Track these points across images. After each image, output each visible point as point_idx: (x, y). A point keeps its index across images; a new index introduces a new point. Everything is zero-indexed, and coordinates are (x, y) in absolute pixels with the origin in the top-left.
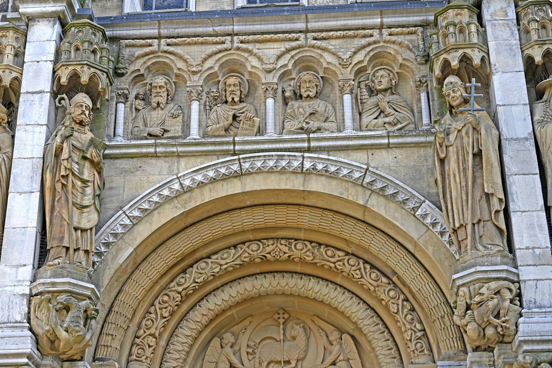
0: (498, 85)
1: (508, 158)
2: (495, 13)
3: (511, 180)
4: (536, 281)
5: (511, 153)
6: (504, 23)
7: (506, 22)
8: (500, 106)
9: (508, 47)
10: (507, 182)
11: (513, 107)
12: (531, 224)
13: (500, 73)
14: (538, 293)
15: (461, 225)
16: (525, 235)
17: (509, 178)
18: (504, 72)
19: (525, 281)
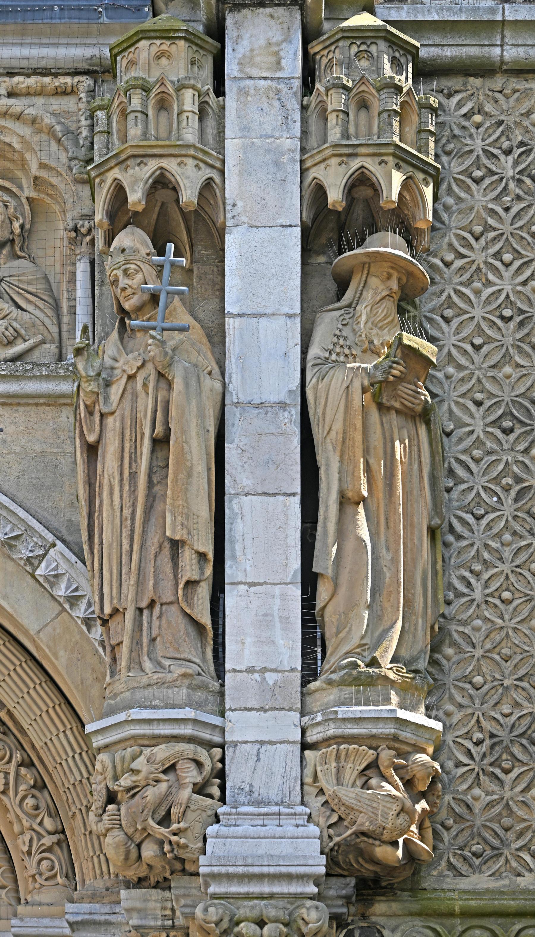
0: (234, 261)
1: (234, 452)
2: (252, 58)
3: (235, 507)
4: (258, 746)
5: (245, 440)
6: (269, 89)
7: (274, 84)
8: (234, 316)
9: (270, 157)
10: (227, 511)
11: (263, 322)
12: (266, 615)
13: (242, 229)
14: (259, 771)
15: (116, 611)
16: (249, 640)
17: (231, 501)
18: (252, 226)
19: (235, 744)
